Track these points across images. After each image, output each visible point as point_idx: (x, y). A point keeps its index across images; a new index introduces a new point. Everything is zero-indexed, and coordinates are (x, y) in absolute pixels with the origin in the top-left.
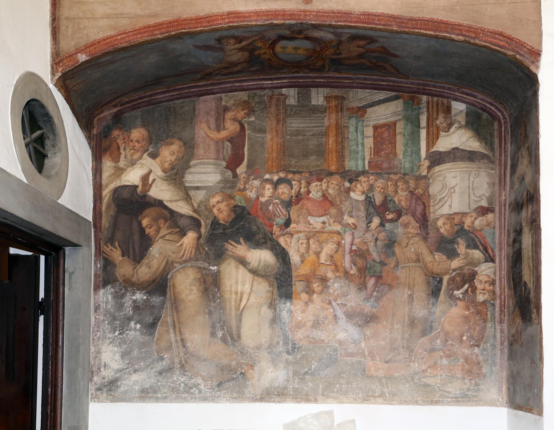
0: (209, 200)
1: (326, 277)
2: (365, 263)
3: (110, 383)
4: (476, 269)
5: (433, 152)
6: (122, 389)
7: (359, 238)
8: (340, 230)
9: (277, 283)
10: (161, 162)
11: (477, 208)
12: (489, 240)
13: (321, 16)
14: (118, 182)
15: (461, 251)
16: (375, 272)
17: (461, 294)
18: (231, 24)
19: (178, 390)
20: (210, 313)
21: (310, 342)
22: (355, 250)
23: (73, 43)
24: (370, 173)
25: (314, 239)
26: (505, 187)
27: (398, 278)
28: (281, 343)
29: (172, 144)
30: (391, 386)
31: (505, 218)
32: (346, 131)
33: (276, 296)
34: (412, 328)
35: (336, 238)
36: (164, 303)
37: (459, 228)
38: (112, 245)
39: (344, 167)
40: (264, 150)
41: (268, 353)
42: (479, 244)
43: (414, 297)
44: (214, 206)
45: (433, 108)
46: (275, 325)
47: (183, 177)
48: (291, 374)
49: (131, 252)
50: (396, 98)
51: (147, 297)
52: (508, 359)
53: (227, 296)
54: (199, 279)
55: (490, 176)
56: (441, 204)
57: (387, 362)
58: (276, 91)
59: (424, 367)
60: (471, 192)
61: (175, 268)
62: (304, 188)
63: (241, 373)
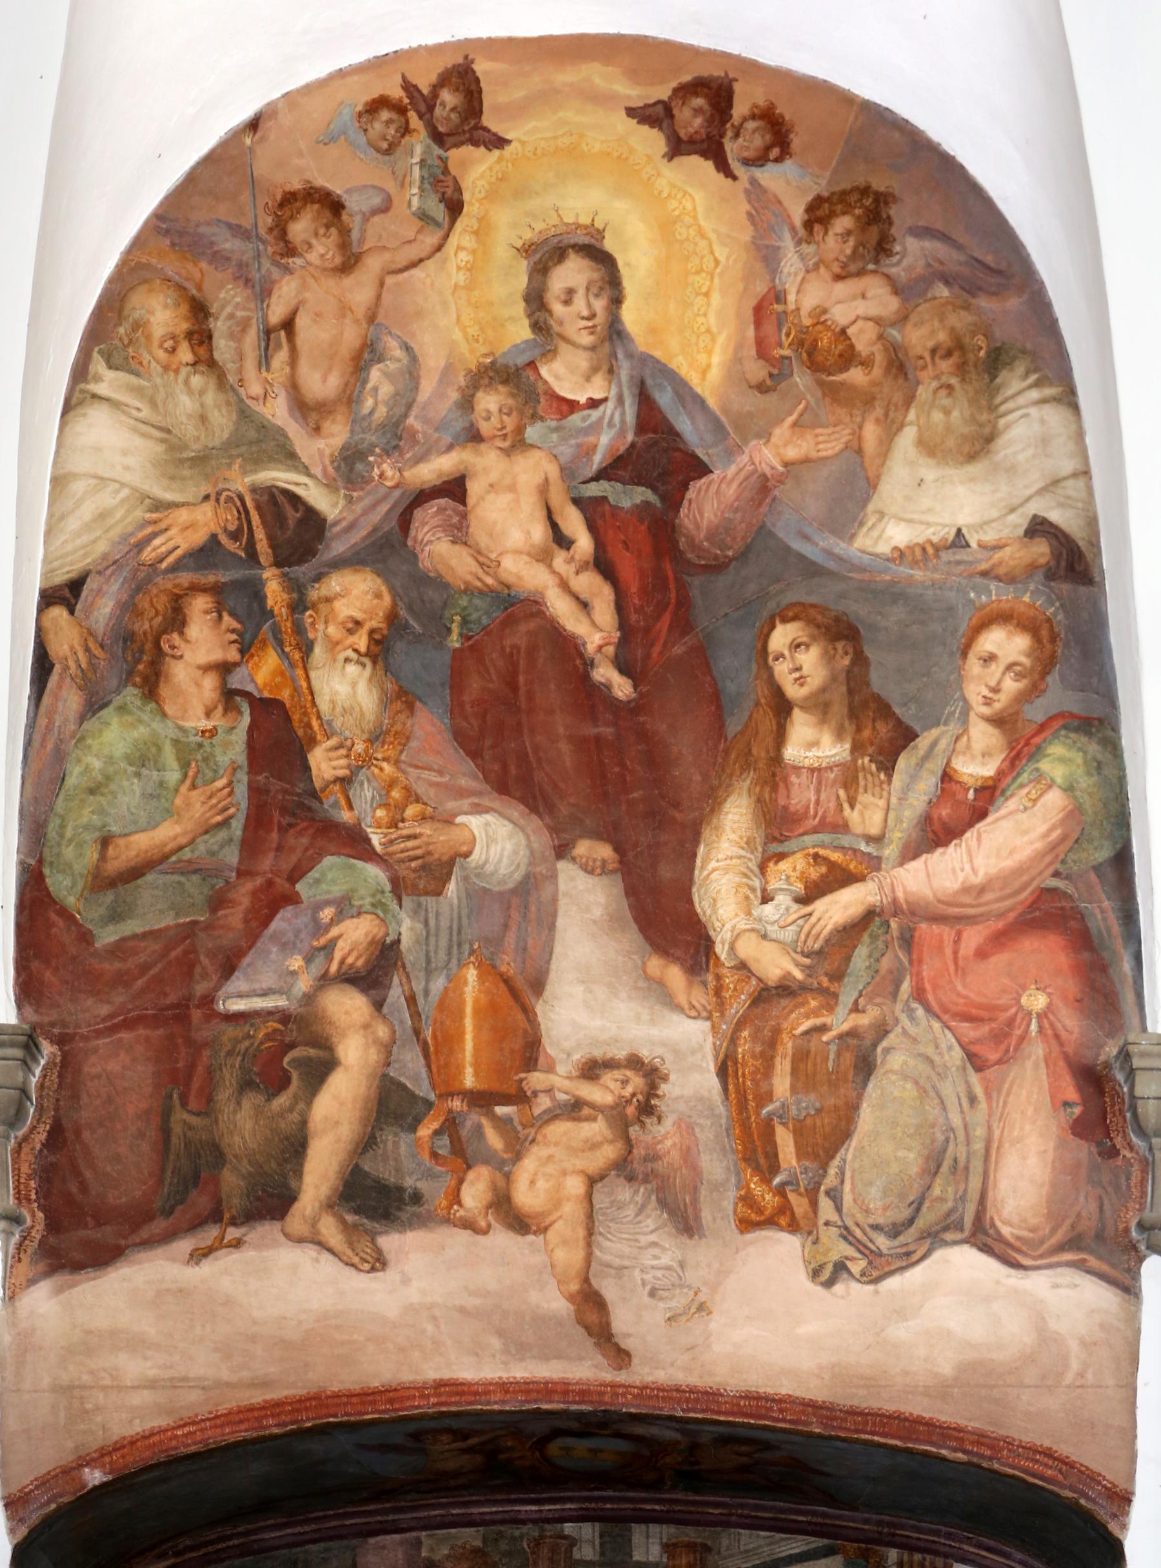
13: (651, 1397)
18: (444, 1409)
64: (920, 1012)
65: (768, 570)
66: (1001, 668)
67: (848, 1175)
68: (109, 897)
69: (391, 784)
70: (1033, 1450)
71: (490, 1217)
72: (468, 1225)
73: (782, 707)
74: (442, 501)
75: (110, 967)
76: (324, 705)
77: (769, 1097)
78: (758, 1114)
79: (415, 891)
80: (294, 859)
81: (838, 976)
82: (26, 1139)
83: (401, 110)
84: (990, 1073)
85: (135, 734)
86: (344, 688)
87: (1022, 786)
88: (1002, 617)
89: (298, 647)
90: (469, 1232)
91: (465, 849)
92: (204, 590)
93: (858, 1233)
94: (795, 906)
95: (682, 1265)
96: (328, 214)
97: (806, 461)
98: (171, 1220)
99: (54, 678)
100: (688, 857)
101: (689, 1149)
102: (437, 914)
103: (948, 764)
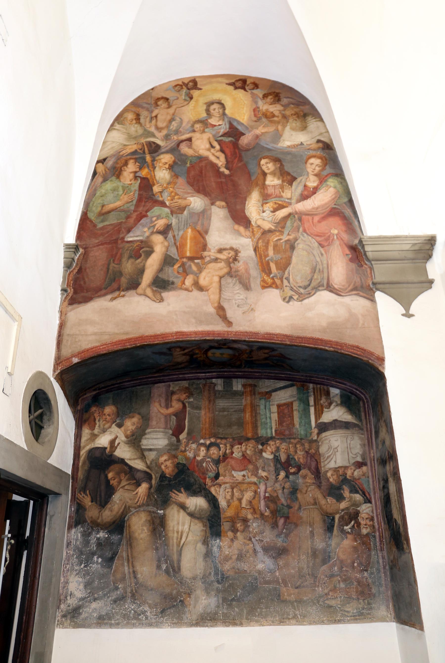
0: (159, 459)
1: (246, 518)
2: (276, 507)
3: (74, 611)
4: (358, 509)
5: (320, 423)
6: (83, 616)
7: (271, 487)
8: (256, 481)
9: (210, 524)
10: (125, 430)
11: (354, 463)
12: (365, 486)
13: (238, 335)
14: (93, 444)
15: (346, 496)
16: (284, 513)
17: (350, 528)
19: (128, 617)
20: (157, 549)
21: (236, 573)
22: (268, 497)
23: (70, 351)
24: (276, 438)
25: (237, 488)
26: (372, 447)
27: (301, 518)
28: (213, 574)
29: (133, 417)
30: (302, 609)
31: (375, 470)
32: (258, 408)
33: (208, 534)
34: (315, 558)
35: (253, 488)
36: (121, 540)
37: (343, 477)
38: (84, 493)
39: (257, 434)
40: (200, 422)
41: (202, 583)
42: (359, 489)
43: (315, 533)
44: (162, 463)
45: (317, 392)
46: (208, 559)
47: (140, 441)
48: (221, 601)
49: (98, 499)
50: (292, 386)
51: (108, 535)
52: (391, 580)
53: (170, 534)
54: (149, 521)
55: (361, 439)
56: (328, 460)
57: (297, 588)
58: (208, 381)
59: (326, 591)
60: (349, 451)
61: (131, 512)
62: (229, 449)
63: (181, 601)
64: (305, 235)
65: (258, 150)
66: (315, 165)
67: (291, 274)
68: (102, 217)
69: (172, 192)
70: (353, 346)
71: (193, 287)
72: (187, 290)
73: (265, 174)
74: (187, 142)
75: (99, 232)
76: (157, 178)
77: (268, 255)
78: (265, 260)
79: (176, 213)
80: (147, 208)
81: (283, 227)
82: (72, 271)
83: (181, 86)
84: (325, 248)
85: (113, 185)
86: (162, 175)
87: (324, 187)
88: (314, 156)
89: (152, 168)
90: (187, 291)
91: (189, 204)
92: (133, 159)
93: (295, 288)
94: (271, 213)
95: (246, 298)
96: (166, 100)
97: (266, 132)
98: (106, 290)
99: (97, 176)
100: (244, 203)
101: (247, 269)
102: (182, 218)
103: (305, 183)
